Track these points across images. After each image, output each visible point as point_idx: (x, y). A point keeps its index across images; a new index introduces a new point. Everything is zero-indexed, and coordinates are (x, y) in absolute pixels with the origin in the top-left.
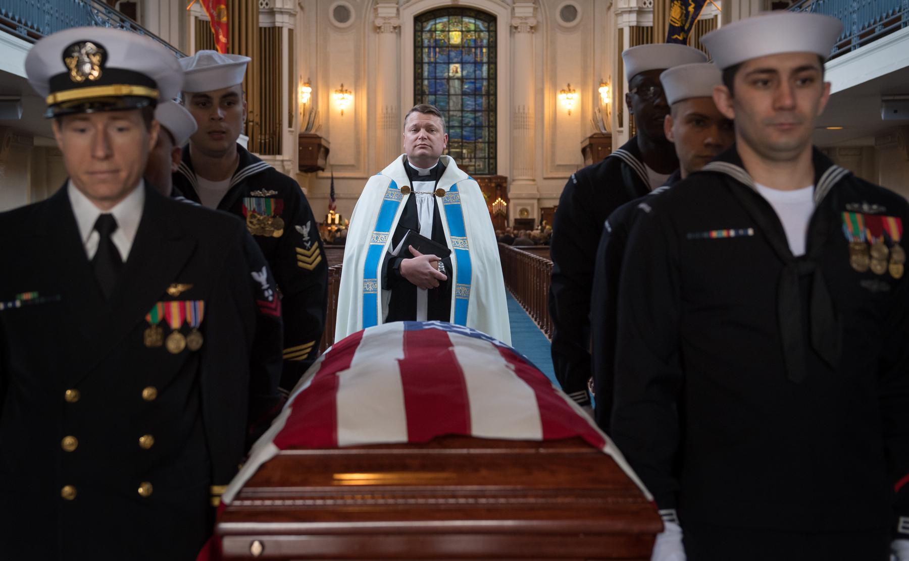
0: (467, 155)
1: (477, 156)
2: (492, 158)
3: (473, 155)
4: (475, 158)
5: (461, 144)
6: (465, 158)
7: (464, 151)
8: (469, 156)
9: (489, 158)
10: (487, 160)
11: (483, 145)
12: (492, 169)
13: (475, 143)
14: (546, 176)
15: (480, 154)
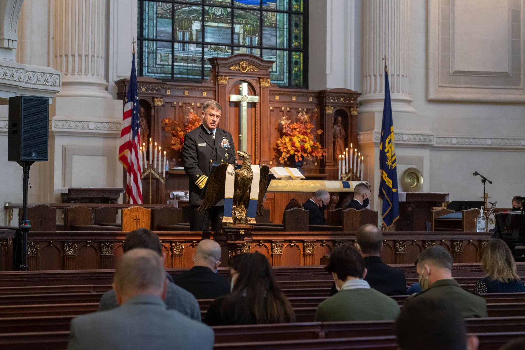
0: (244, 39)
1: (265, 43)
2: (297, 50)
3: (256, 40)
4: (260, 47)
5: (229, 10)
6: (239, 46)
7: (238, 28)
8: (248, 42)
9: (290, 50)
10: (286, 53)
11: (279, 16)
12: (297, 75)
13: (261, 10)
14: (432, 96)
15: (270, 39)
